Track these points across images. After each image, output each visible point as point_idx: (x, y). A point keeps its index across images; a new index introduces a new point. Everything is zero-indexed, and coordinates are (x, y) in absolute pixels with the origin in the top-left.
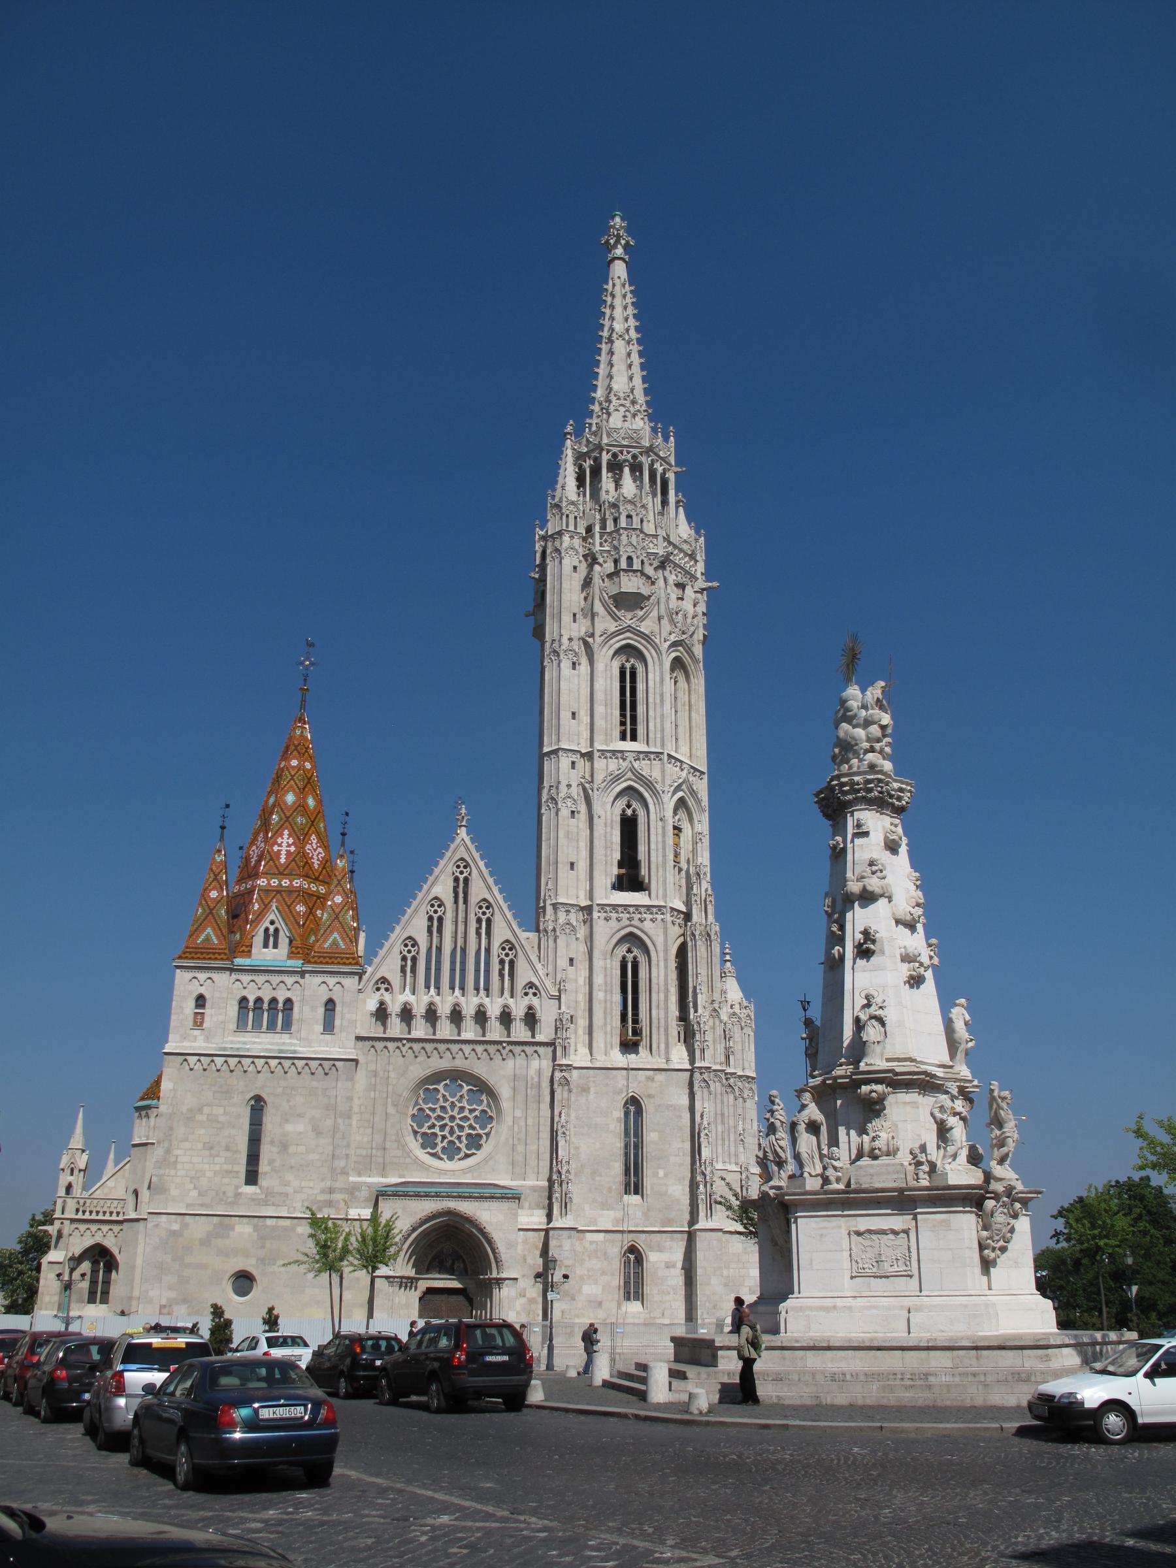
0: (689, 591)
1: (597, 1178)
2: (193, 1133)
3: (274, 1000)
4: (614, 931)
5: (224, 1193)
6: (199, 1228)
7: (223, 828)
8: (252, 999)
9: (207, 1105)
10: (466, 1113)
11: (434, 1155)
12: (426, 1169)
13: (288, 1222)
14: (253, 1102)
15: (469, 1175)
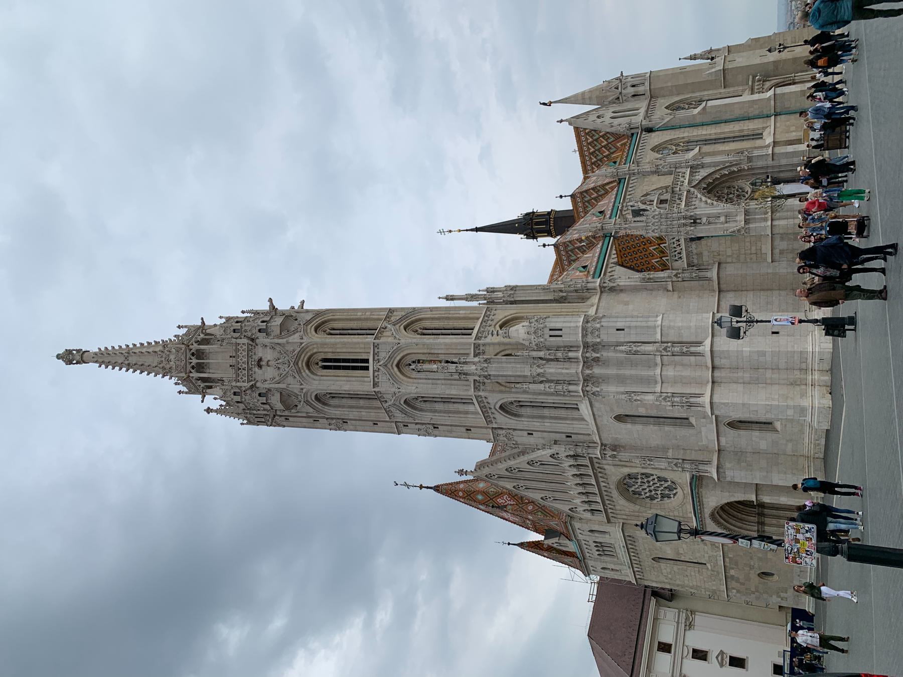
0: (260, 352)
1: (678, 437)
2: (679, 579)
3: (595, 546)
4: (501, 416)
5: (712, 574)
6: (733, 584)
7: (509, 544)
8: (598, 553)
9: (662, 574)
10: (645, 480)
11: (675, 495)
12: (684, 503)
13: (727, 560)
14: (657, 559)
15: (686, 489)
